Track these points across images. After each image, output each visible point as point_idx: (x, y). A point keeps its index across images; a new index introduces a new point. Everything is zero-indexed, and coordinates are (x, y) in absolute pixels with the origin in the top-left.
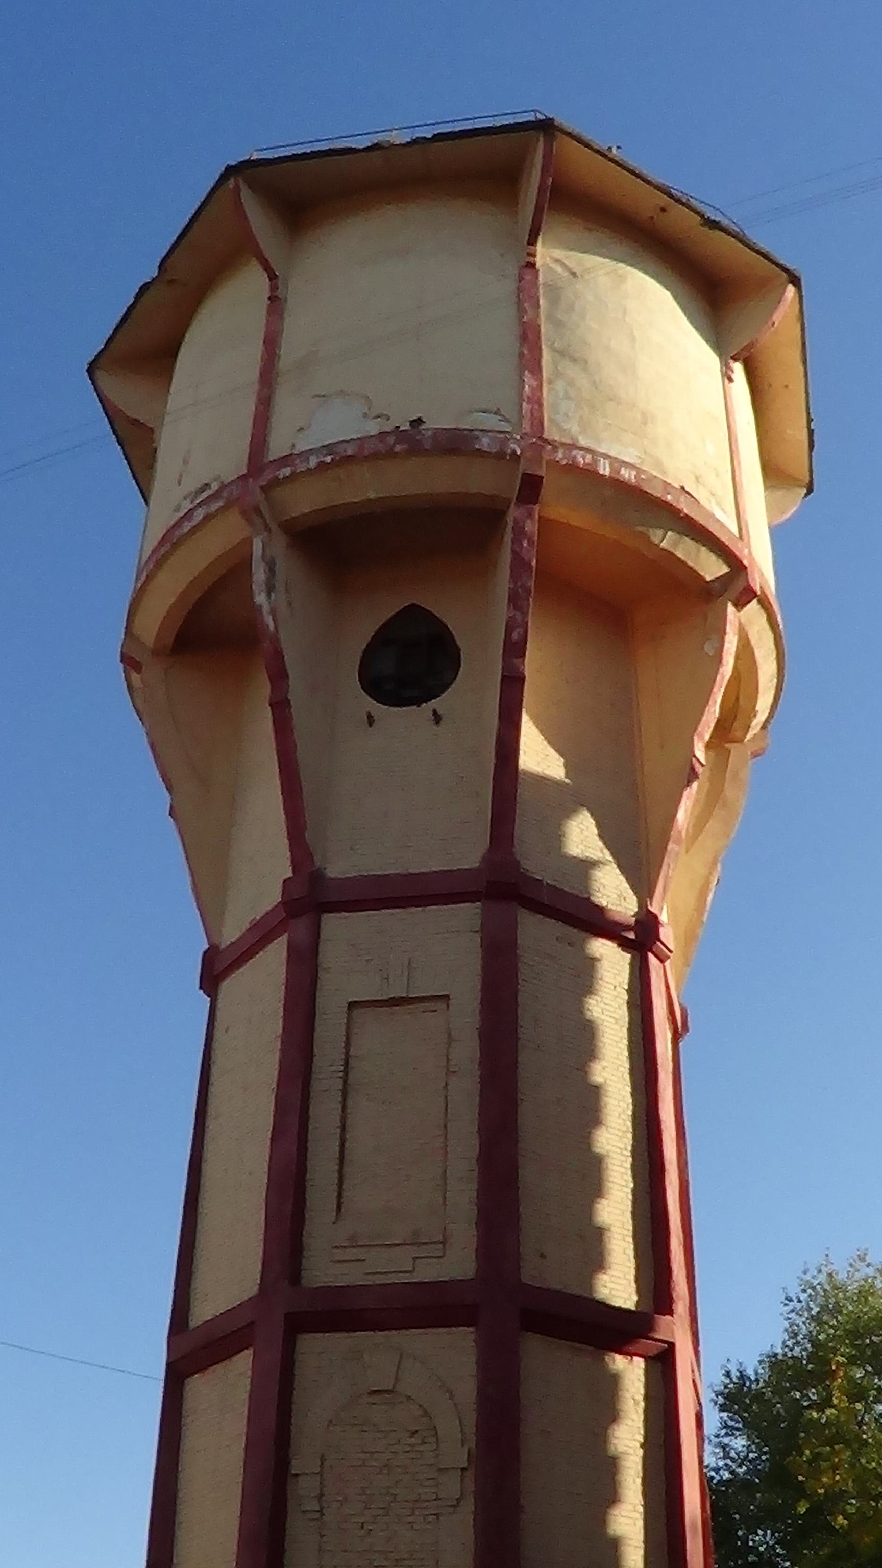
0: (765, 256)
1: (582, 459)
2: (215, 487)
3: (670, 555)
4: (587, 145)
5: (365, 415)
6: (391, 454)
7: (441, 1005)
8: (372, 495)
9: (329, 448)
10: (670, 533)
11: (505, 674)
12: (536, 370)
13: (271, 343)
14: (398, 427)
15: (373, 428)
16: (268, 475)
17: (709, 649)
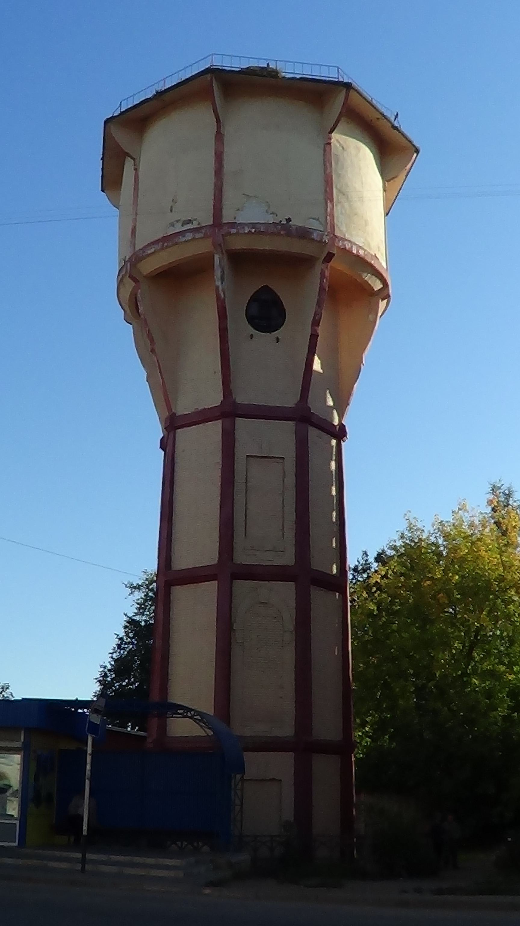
0: (410, 142)
1: (348, 246)
2: (195, 225)
3: (366, 282)
4: (361, 95)
5: (267, 212)
6: (279, 234)
7: (283, 459)
8: (267, 248)
9: (253, 225)
10: (369, 274)
11: (313, 333)
12: (332, 201)
13: (219, 157)
14: (281, 221)
15: (271, 220)
16: (225, 229)
17: (371, 317)
